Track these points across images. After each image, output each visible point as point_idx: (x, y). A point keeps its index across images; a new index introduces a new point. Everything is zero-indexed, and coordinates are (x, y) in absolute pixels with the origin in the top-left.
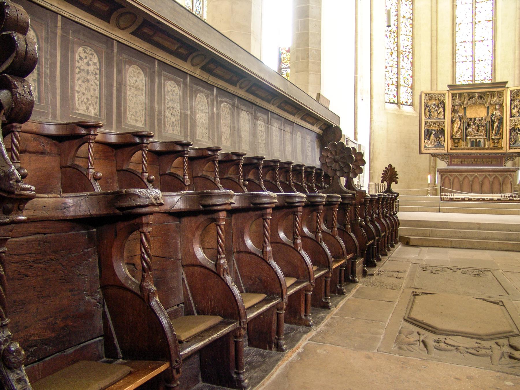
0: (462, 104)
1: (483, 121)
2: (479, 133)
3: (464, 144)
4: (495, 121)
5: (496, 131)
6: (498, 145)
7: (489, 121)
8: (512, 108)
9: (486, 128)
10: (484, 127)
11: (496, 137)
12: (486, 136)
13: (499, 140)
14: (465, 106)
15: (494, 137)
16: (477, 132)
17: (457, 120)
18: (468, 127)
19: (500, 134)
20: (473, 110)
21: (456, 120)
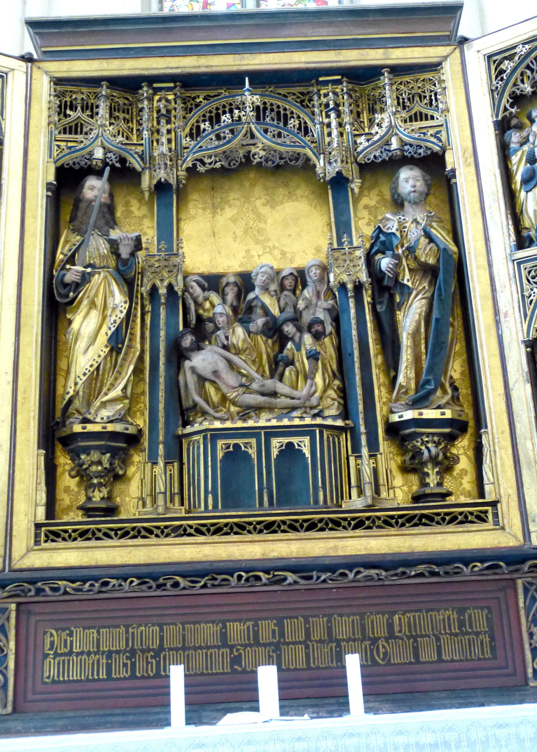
0: (136, 164)
1: (308, 293)
2: (282, 388)
3: (161, 487)
4: (406, 279)
5: (417, 359)
6: (449, 484)
7: (358, 287)
8: (518, 178)
9: (339, 349)
10: (318, 336)
11: (430, 414)
12: (345, 414)
13: (451, 438)
14: (162, 175)
15: (409, 415)
16: (271, 384)
17: (96, 279)
18: (188, 341)
19: (455, 389)
20: (229, 212)
21: (85, 278)
